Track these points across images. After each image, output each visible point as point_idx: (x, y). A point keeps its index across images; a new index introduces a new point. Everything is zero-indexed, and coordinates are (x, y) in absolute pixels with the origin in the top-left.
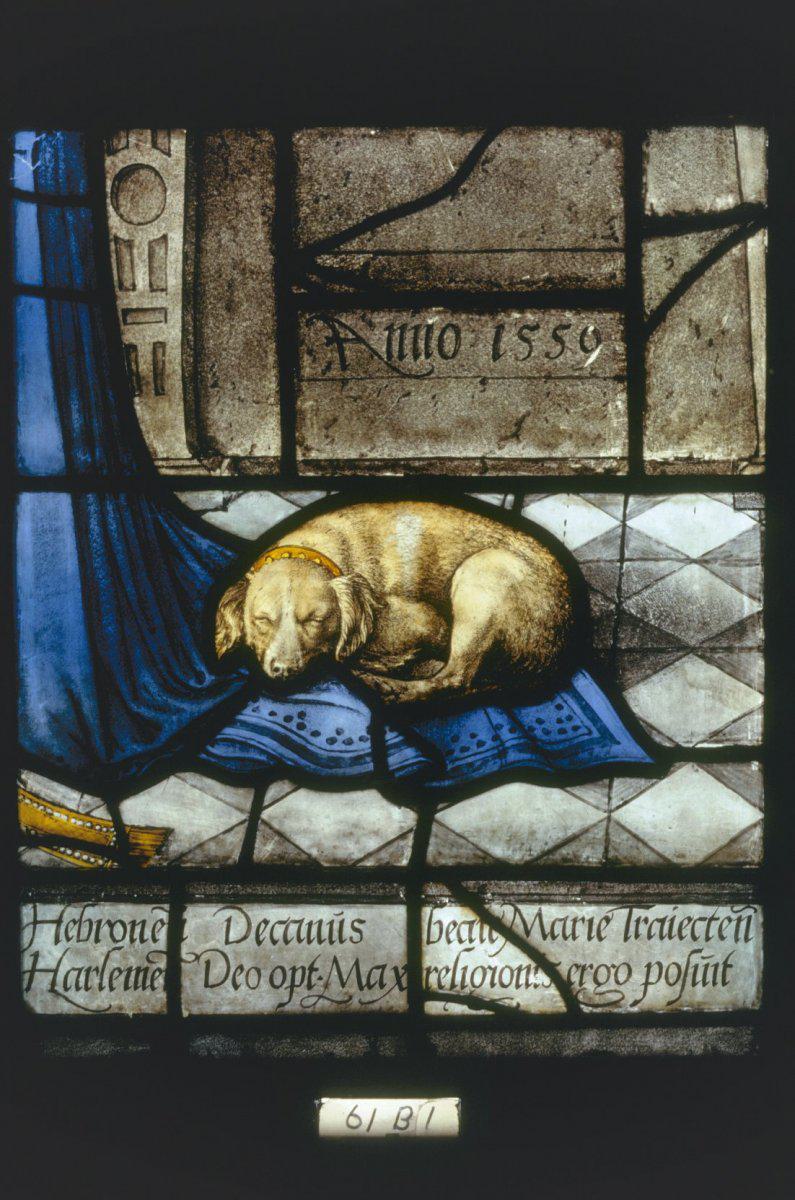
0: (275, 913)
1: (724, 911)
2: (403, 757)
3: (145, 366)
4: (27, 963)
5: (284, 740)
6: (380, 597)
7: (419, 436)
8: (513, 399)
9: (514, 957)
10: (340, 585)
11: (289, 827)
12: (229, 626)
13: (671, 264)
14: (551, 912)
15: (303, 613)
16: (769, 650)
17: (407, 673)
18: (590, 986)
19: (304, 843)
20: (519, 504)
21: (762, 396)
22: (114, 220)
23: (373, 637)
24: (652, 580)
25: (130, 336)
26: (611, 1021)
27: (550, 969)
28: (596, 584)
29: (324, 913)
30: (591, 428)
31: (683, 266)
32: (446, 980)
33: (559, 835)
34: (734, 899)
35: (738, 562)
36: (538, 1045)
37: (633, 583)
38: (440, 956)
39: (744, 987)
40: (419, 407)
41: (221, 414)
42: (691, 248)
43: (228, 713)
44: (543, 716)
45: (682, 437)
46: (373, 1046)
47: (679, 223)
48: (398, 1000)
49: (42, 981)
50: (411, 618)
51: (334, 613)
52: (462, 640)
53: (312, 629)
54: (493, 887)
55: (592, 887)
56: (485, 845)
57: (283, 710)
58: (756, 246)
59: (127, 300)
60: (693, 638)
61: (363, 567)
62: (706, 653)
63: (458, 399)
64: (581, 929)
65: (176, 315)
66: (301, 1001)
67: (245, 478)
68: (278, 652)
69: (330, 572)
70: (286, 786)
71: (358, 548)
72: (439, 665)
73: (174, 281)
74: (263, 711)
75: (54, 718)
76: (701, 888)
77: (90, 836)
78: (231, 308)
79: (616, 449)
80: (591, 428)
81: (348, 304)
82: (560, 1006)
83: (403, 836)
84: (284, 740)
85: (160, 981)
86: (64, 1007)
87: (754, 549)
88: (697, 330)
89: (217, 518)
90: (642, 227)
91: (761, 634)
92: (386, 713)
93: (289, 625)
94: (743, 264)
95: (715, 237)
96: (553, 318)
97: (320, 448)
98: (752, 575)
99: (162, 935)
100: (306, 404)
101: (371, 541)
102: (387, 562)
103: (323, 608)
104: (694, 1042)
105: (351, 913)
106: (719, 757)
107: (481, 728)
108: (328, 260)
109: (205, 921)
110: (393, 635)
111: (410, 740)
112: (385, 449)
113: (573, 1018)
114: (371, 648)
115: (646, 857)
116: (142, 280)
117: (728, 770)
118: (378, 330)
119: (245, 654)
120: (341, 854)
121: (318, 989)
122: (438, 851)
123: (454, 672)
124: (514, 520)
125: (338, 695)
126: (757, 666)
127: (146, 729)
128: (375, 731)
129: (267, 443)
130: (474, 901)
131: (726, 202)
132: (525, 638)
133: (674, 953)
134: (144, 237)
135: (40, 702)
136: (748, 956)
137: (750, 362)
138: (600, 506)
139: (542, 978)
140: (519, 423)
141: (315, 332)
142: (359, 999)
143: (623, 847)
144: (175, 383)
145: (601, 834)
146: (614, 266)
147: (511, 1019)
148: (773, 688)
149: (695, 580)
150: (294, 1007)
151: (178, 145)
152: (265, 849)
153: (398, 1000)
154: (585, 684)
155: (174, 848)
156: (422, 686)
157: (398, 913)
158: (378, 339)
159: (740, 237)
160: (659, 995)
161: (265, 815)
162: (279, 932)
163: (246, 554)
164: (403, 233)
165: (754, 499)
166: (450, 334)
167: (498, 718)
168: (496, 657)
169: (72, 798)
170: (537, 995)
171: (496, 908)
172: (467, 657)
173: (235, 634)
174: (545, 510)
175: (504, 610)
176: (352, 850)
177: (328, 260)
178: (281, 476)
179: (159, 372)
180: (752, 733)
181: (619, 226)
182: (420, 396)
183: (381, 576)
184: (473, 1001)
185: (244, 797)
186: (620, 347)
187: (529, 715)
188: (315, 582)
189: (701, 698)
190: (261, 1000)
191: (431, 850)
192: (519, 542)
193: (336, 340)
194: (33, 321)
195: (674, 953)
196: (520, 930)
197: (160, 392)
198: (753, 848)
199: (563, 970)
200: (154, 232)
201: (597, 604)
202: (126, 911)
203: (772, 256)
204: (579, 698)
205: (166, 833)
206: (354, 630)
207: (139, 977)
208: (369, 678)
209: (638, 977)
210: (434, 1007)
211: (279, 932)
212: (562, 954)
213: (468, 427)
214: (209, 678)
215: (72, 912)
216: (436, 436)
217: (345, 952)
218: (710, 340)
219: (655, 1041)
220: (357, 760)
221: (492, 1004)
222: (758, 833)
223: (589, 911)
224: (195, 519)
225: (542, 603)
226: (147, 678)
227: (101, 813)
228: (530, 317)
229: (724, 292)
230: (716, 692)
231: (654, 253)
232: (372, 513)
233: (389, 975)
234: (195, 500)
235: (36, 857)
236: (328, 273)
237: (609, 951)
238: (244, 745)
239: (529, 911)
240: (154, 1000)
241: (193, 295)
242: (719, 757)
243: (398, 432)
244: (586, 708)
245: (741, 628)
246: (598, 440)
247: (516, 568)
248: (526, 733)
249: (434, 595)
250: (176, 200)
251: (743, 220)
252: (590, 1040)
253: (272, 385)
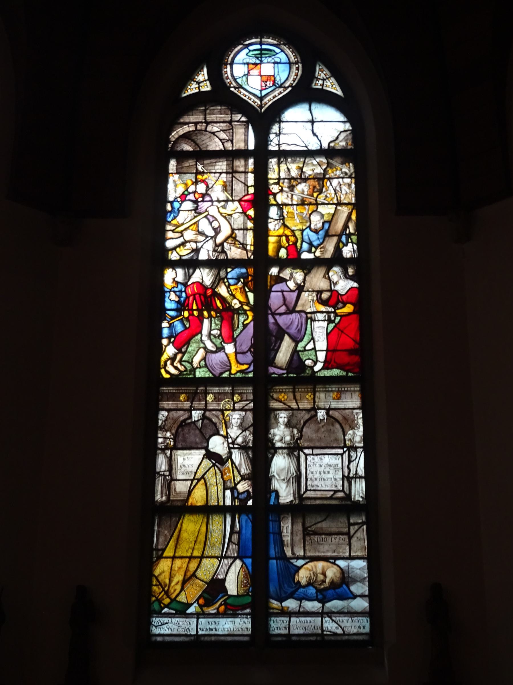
0: (303, 619)
1: (364, 618)
2: (320, 596)
3: (285, 543)
4: (269, 626)
5: (304, 594)
6: (317, 574)
7: (321, 552)
8: (334, 547)
9: (336, 625)
10: (311, 572)
11: (305, 606)
12: (297, 578)
13: (354, 529)
14: (341, 619)
15: (307, 576)
16: (369, 581)
17: (320, 585)
18: (346, 629)
19: (307, 609)
20: (335, 561)
21: (366, 547)
22: (282, 523)
23: (316, 580)
24: (353, 572)
25: (284, 539)
26: (349, 635)
27: (341, 627)
28: (345, 572)
29: (310, 619)
30: (344, 551)
31: (355, 530)
32: (327, 629)
33: (341, 608)
34: (365, 617)
35: (364, 569)
36: (339, 638)
37: (350, 572)
38: (325, 625)
39: (367, 630)
40: (321, 548)
41: (295, 550)
42: (356, 527)
43: (297, 590)
44: (339, 591)
45: (356, 552)
46: (317, 638)
47: (354, 524)
48: (320, 631)
49: (271, 629)
50: (321, 577)
51: (311, 576)
52: (328, 580)
53: (308, 578)
54: (333, 615)
55: (346, 615)
56: (331, 609)
57: (304, 590)
58: (365, 527)
59: (283, 534)
60: (358, 580)
61: (314, 570)
62: (360, 582)
63: (326, 547)
64: (345, 621)
65: (290, 536)
66: (307, 632)
67: (298, 558)
68: (303, 582)
69: (310, 571)
70: (304, 601)
71: (314, 567)
72: (325, 583)
73: (289, 531)
74: (301, 590)
75: (273, 591)
76: (361, 615)
77: (278, 608)
78: (297, 535)
79: (347, 554)
80: (344, 551)
81: (312, 534)
82: (342, 632)
83: (320, 608)
84: (304, 594)
85: (287, 629)
86: (274, 633)
87: (366, 568)
88: (357, 538)
89: (295, 563)
90: (350, 525)
91: (367, 579)
92: (318, 590)
93: (305, 578)
94: (363, 529)
95: (359, 526)
96: (339, 536)
97: (309, 554)
98: (366, 571)
99: (288, 622)
100: (307, 548)
101: (316, 567)
102: (318, 569)
103: (309, 576)
104: (361, 638)
105: (313, 619)
106: (362, 596)
107: (330, 592)
108: (309, 529)
109: (293, 620)
110: (318, 579)
111: (321, 594)
112: (317, 554)
113: (344, 634)
114: (316, 581)
115: (353, 611)
116: (285, 531)
117: (364, 598)
118: (316, 538)
119: (299, 582)
120: (312, 611)
121: (309, 630)
122: (325, 610)
123: (327, 585)
124: (334, 563)
125: (311, 588)
126: (367, 584)
127: (285, 593)
128: (316, 593)
129: (302, 553)
130: (330, 617)
131: (361, 521)
132: (336, 580)
133: (358, 624)
134: (285, 526)
135: (272, 588)
136: (368, 625)
137: (365, 542)
138: (346, 562)
139: (340, 628)
140: (335, 550)
141: (308, 538)
142: (315, 631)
143: (350, 609)
144: (290, 545)
145: (347, 607)
146: (346, 530)
147: (335, 634)
148: (370, 586)
149: (358, 572)
150: (306, 633)
151: (290, 514)
152: (302, 610)
153: (320, 631)
154: (344, 586)
155: (289, 610)
156: (322, 587)
157: (320, 619)
158: (316, 539)
159: (363, 526)
160: (356, 631)
161: (302, 605)
162: (304, 622)
163: (299, 568)
164: (319, 525)
165: (366, 561)
166: (325, 539)
167: (333, 591)
168: (332, 582)
169: (275, 602)
170: (339, 631)
171: (333, 618)
172: (329, 583)
173: (298, 579)
174: (338, 562)
175: (333, 576)
176: (313, 610)
177: (309, 529)
178: (304, 558)
179: (287, 543)
180: (367, 593)
181: (347, 525)
182: (322, 547)
183: (317, 571)
184: (330, 632)
185: (299, 602)
186: (348, 540)
187: (337, 590)
188: (308, 572)
189: (360, 588)
190: (301, 632)
191: (324, 610)
192: (335, 567)
193: (310, 539)
194: (272, 537)
195: (358, 624)
196: (336, 621)
197: (288, 546)
198: (368, 609)
199: (343, 627)
200: (287, 525)
201: (346, 575)
202: (283, 619)
203: (367, 528)
204: (343, 588)
205: (288, 607)
206: (313, 579)
207: (285, 628)
208: (315, 586)
209: (353, 628)
210: (325, 633)
211: (304, 622)
212: (343, 625)
213: (328, 551)
214: (294, 585)
215: (275, 619)
216: (324, 552)
217: (313, 625)
218: (359, 539)
219: (355, 637)
220: (314, 597)
221: (333, 632)
222: (368, 607)
223: (346, 618)
224: (292, 563)
225: (338, 575)
226: (286, 586)
227: (280, 604)
228: (336, 536)
229: (361, 533)
230: (362, 588)
231: (352, 528)
232: (315, 563)
233: (319, 628)
234: (292, 561)
235: (272, 611)
236: (309, 531)
237: (348, 624)
238: (299, 595)
239: (338, 618)
240: (286, 632)
241: (292, 533)
242: (362, 596)
243: (319, 552)
244: (344, 589)
245: (365, 578)
246: (345, 553)
247: (335, 570)
248: (337, 593)
249: (324, 574)
250: (290, 521)
251: (363, 523)
252: (346, 637)
253: (302, 545)
